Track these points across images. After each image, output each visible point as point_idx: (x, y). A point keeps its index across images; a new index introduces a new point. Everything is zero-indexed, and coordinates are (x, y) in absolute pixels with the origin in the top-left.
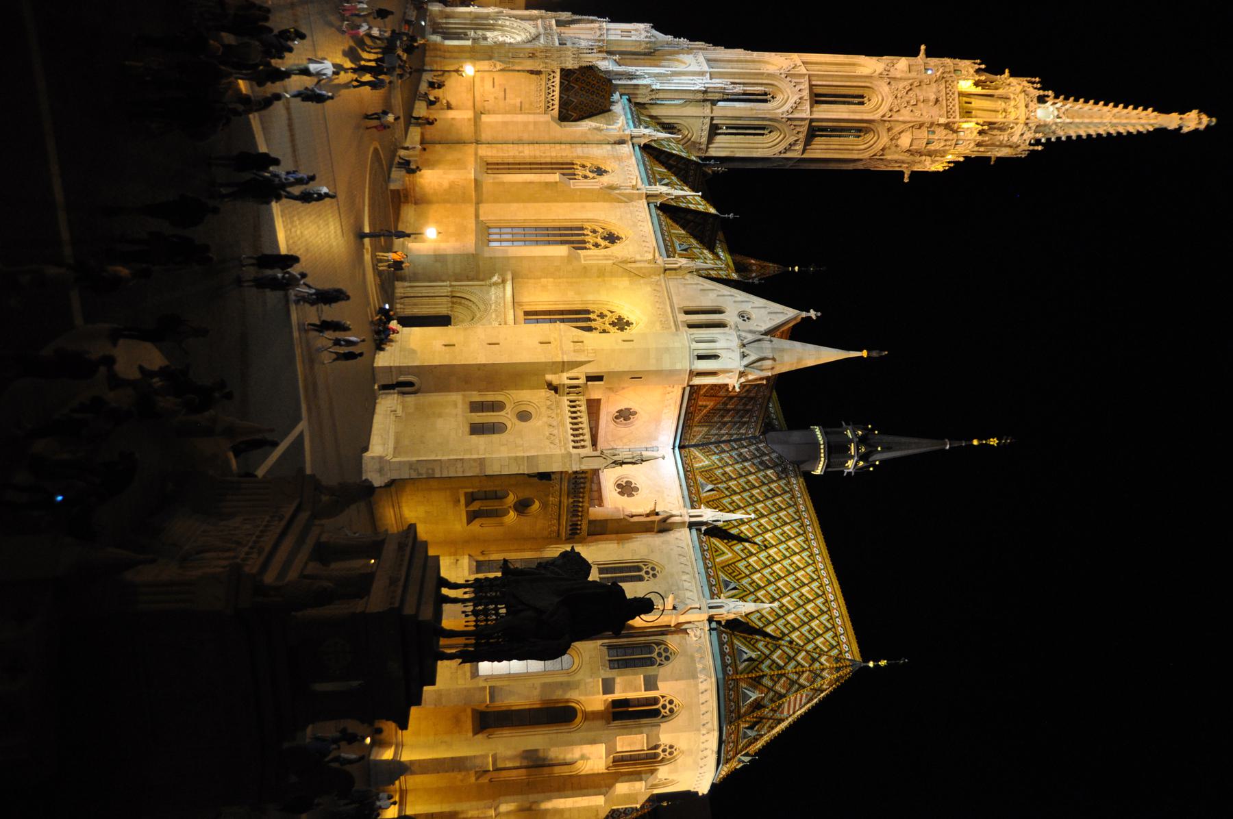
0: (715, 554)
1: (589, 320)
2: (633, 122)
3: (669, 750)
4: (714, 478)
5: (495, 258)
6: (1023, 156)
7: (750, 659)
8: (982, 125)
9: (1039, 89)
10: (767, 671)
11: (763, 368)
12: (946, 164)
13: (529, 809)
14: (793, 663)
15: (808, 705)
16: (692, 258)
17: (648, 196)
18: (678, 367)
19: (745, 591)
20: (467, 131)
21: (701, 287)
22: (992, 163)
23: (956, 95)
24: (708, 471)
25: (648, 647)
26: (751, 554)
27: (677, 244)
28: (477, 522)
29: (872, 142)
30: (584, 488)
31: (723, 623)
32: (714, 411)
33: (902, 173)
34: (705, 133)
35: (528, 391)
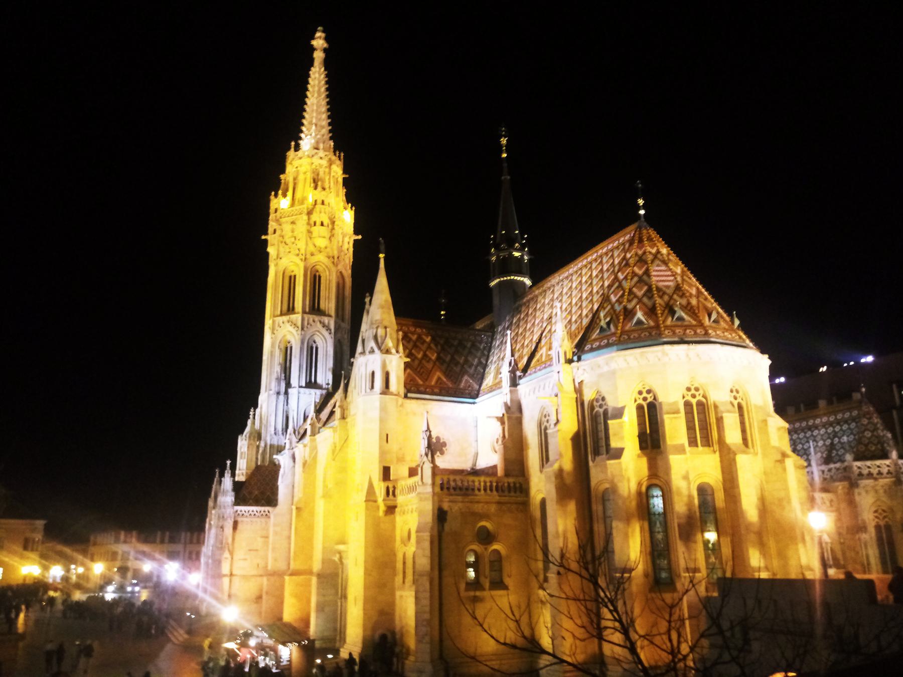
3: (693, 392)
10: (622, 306)
11: (383, 334)
18: (377, 404)
28: (508, 581)
29: (324, 266)
32: (448, 374)
33: (355, 241)
34: (313, 391)
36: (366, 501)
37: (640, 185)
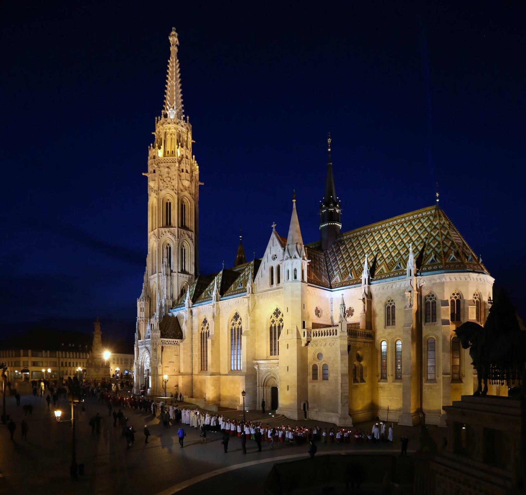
0: (383, 273)
1: (275, 327)
4: (345, 273)
6: (191, 126)
9: (161, 117)
17: (217, 301)
19: (401, 260)
21: (261, 276)
23: (165, 158)
24: (342, 276)
25: (427, 304)
26: (382, 257)
27: (238, 288)
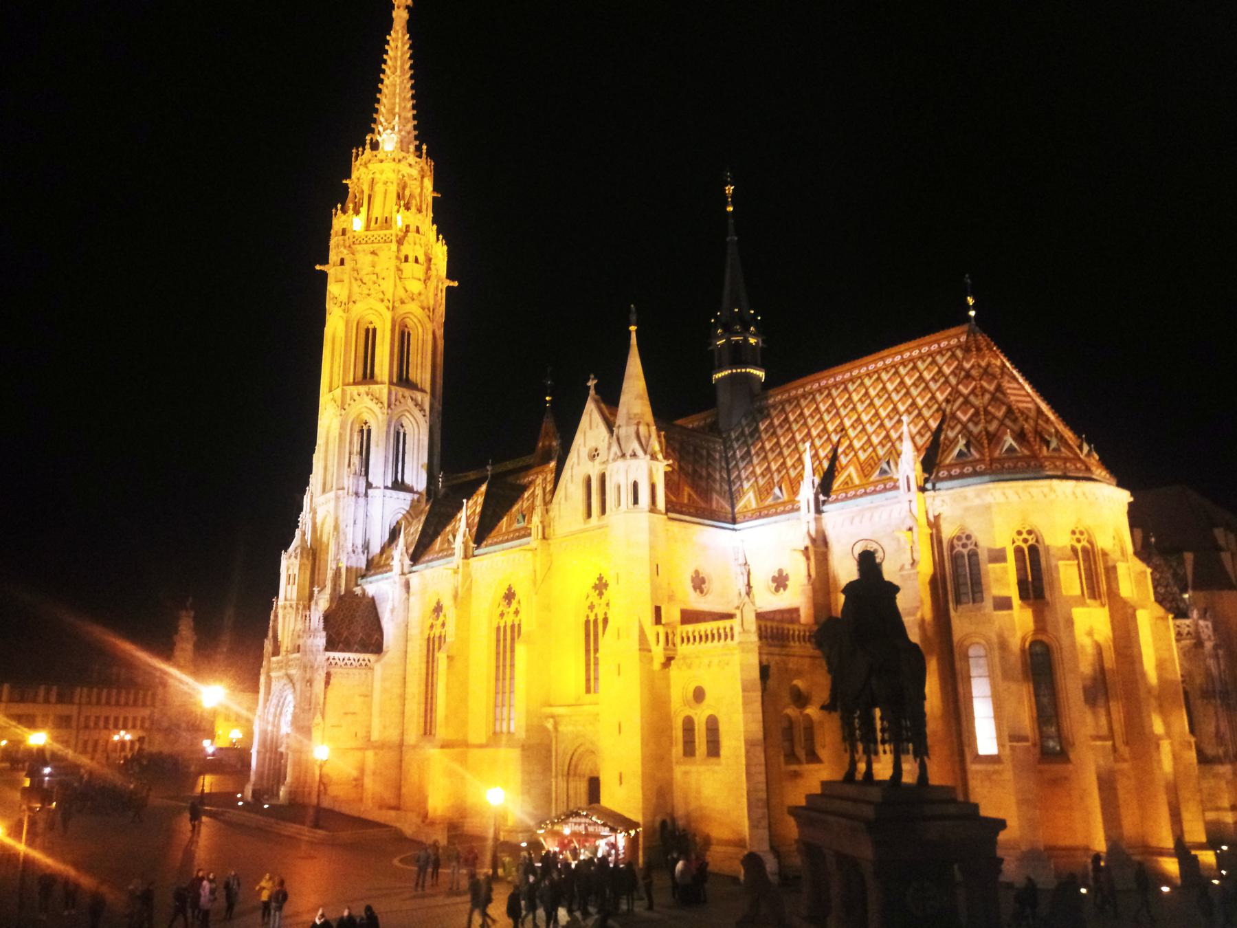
1: (596, 621)
2: (386, 572)
5: (527, 725)
6: (433, 164)
7: (967, 445)
8: (400, 207)
9: (364, 149)
10: (980, 427)
11: (647, 434)
12: (440, 242)
13: (1159, 698)
14: (972, 398)
15: (1021, 380)
16: (532, 509)
17: (466, 557)
19: (891, 453)
20: (390, 756)
22: (439, 196)
26: (851, 446)
27: (517, 526)
29: (415, 320)
30: (777, 629)
31: (927, 476)
32: (695, 486)
33: (448, 288)
34: (402, 495)
35: (672, 690)
36: (640, 650)
37: (969, 281)
